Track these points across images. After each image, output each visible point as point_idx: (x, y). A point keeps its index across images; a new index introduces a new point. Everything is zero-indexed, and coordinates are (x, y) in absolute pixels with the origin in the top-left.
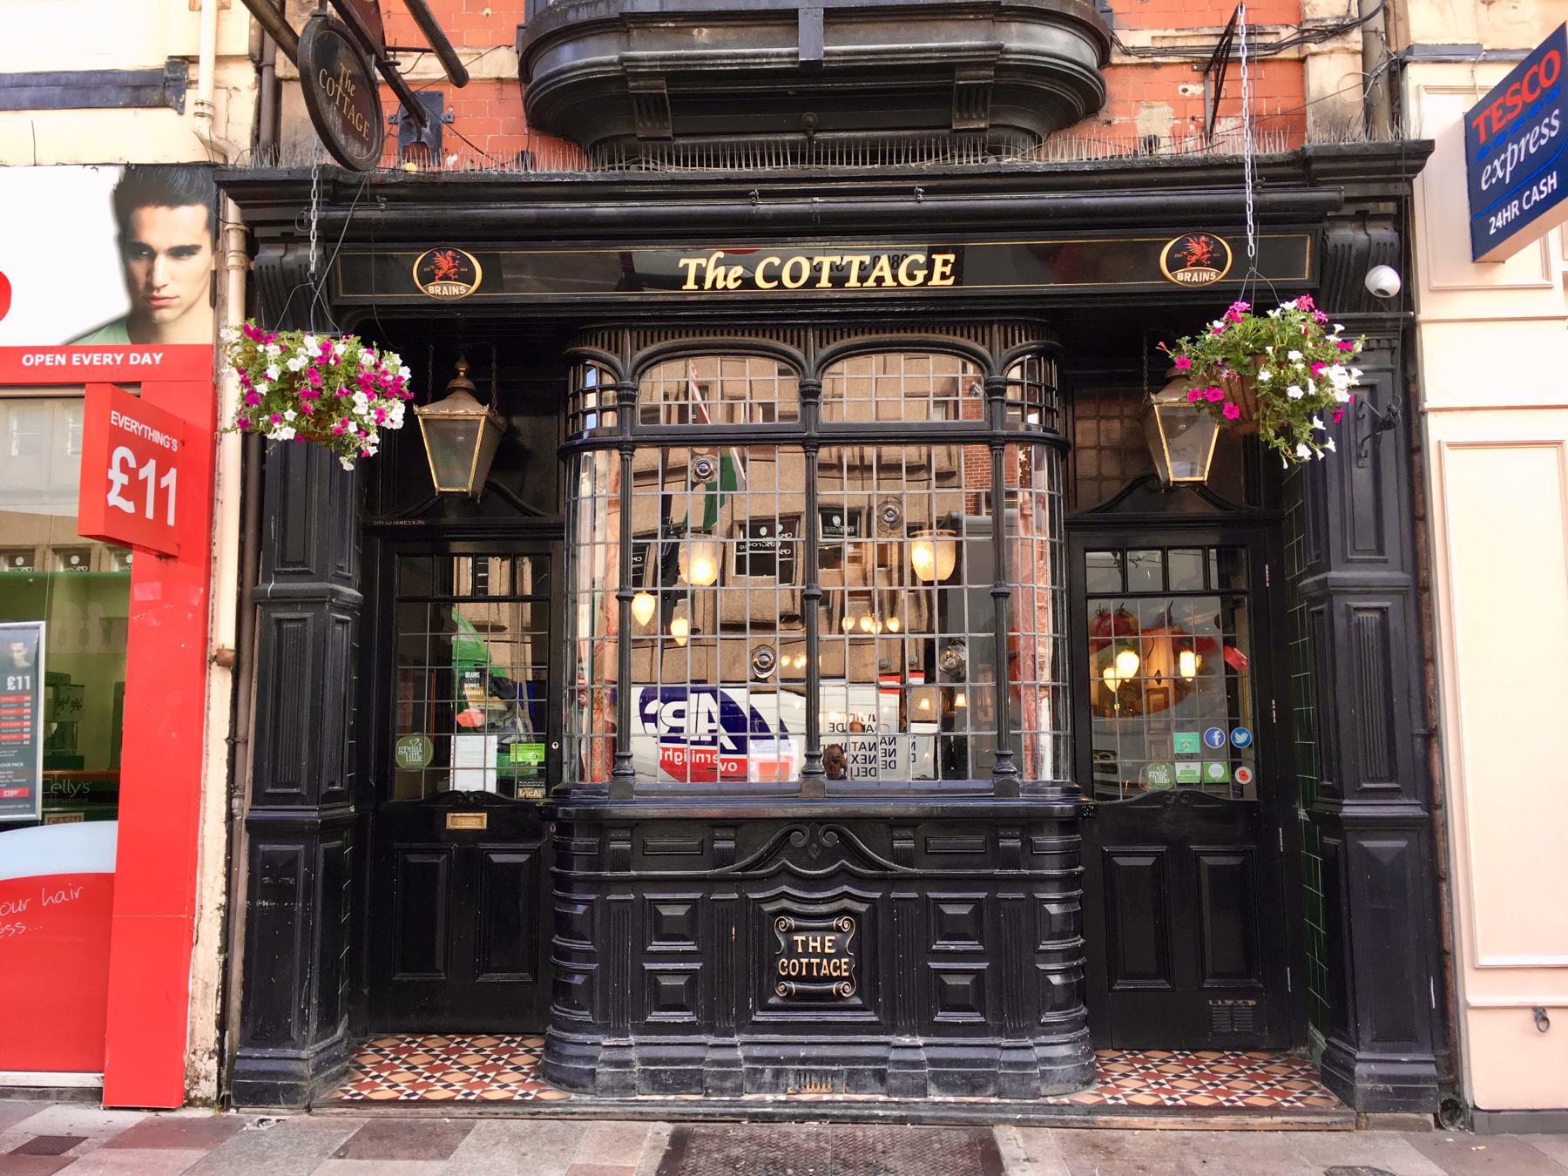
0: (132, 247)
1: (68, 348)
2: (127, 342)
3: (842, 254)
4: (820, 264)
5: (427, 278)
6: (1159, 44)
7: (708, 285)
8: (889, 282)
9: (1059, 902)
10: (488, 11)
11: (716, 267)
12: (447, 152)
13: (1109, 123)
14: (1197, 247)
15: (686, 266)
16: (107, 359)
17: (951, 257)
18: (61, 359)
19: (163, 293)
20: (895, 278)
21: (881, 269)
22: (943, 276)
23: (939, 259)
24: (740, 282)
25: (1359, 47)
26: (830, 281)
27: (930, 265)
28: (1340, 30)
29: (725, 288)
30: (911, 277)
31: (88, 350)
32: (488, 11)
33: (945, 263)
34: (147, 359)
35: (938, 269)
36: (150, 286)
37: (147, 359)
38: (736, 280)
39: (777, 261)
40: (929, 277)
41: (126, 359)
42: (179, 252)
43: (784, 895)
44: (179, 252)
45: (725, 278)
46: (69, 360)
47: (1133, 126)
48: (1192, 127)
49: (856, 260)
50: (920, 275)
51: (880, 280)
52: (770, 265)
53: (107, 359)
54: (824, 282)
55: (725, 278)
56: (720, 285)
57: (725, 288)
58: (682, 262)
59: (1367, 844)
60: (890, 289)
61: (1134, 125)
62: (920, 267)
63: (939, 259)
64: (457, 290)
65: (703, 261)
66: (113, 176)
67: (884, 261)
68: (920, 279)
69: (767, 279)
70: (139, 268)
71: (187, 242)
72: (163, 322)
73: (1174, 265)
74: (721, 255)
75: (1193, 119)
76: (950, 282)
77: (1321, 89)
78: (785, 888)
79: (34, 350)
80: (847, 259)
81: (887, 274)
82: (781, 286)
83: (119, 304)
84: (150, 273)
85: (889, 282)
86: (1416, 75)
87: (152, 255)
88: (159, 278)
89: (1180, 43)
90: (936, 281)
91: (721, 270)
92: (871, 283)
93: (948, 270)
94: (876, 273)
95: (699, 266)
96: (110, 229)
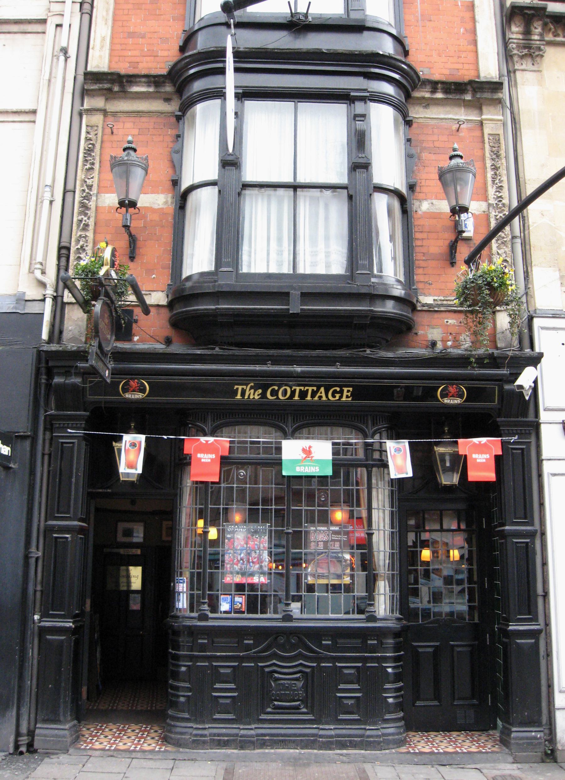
3: (304, 386)
4: (295, 390)
5: (125, 390)
7: (246, 397)
8: (324, 398)
9: (393, 668)
10: (154, 276)
11: (250, 390)
12: (134, 335)
13: (416, 334)
14: (452, 389)
15: (238, 389)
17: (351, 389)
20: (327, 396)
21: (321, 393)
22: (347, 397)
23: (345, 389)
24: (260, 396)
26: (299, 397)
27: (341, 392)
29: (254, 398)
30: (334, 396)
32: (154, 276)
33: (348, 391)
35: (345, 393)
38: (258, 395)
39: (276, 388)
40: (341, 397)
43: (274, 665)
45: (254, 395)
47: (426, 335)
48: (450, 337)
49: (310, 389)
50: (338, 396)
51: (320, 397)
52: (274, 389)
54: (296, 398)
55: (254, 395)
56: (251, 397)
57: (254, 398)
58: (236, 387)
59: (518, 641)
60: (325, 401)
61: (427, 335)
62: (338, 393)
63: (345, 389)
64: (139, 396)
65: (245, 387)
67: (322, 389)
68: (337, 398)
69: (272, 395)
73: (443, 396)
74: (252, 384)
75: (451, 334)
76: (350, 399)
78: (274, 661)
80: (306, 388)
81: (323, 395)
82: (278, 398)
85: (324, 398)
86: (537, 322)
89: (445, 302)
90: (344, 399)
91: (252, 391)
92: (316, 398)
93: (349, 394)
94: (319, 394)
95: (243, 389)
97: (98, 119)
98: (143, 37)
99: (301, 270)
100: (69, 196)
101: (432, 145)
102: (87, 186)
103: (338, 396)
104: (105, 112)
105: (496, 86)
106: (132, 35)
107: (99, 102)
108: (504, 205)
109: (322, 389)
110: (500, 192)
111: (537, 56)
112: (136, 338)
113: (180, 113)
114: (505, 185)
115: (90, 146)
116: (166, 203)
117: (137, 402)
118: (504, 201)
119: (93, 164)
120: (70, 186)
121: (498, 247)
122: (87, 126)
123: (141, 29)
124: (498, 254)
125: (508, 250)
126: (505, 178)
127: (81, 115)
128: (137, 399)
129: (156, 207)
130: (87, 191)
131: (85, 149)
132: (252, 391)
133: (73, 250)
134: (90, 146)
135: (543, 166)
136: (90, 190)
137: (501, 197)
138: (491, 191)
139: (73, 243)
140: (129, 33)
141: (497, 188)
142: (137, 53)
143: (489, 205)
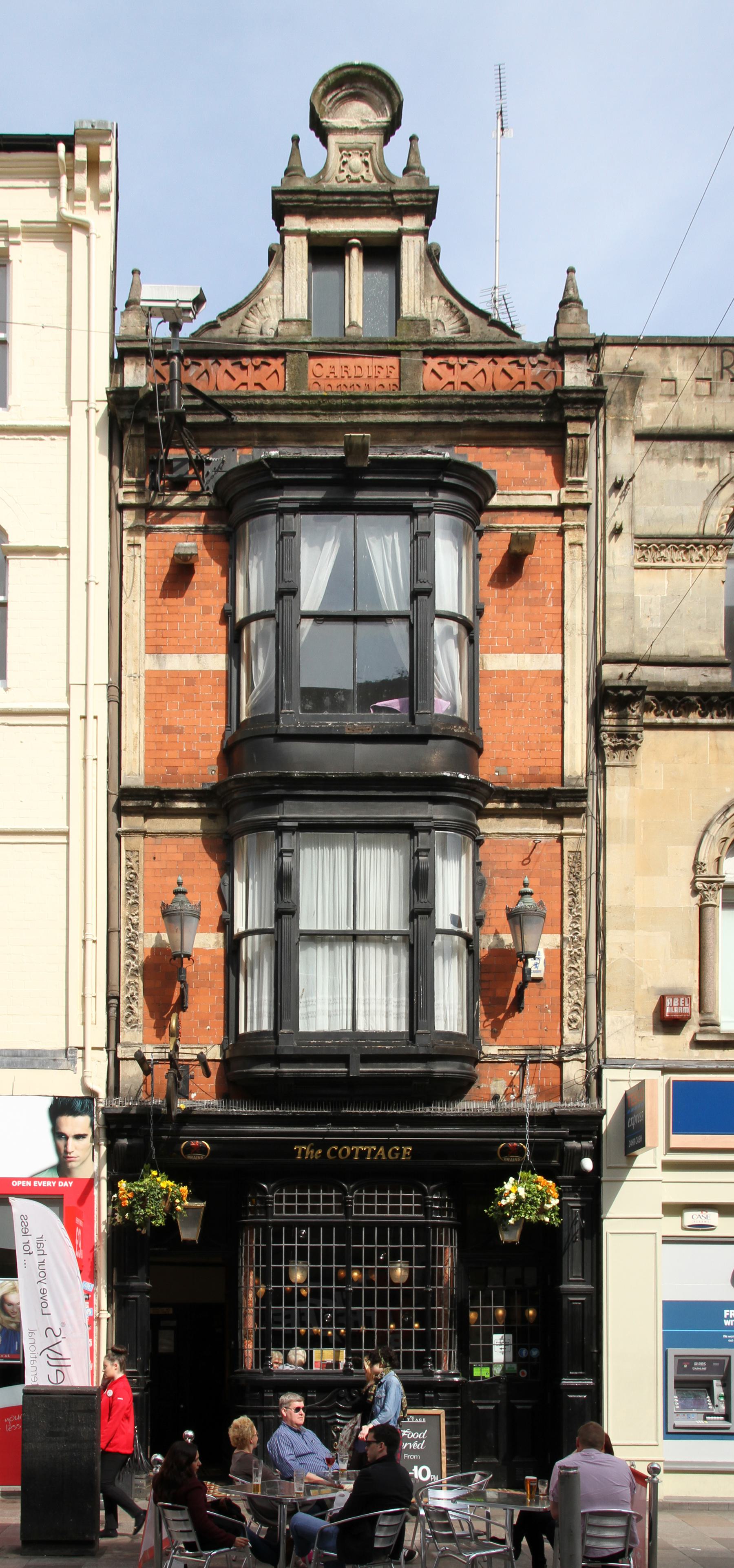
0: (58, 1134)
1: (31, 1179)
2: (57, 1176)
6: (501, 1052)
8: (384, 1158)
10: (208, 1027)
16: (49, 1184)
18: (29, 1183)
19: (72, 1155)
25: (585, 1059)
28: (577, 1051)
31: (40, 1180)
32: (208, 1027)
34: (66, 1184)
36: (66, 1152)
37: (66, 1184)
40: (401, 1156)
41: (57, 1184)
42: (78, 1137)
44: (78, 1137)
46: (32, 1184)
47: (489, 1089)
50: (397, 1155)
51: (380, 1156)
53: (49, 1184)
66: (49, 1102)
67: (381, 1149)
68: (397, 1157)
70: (61, 1143)
71: (82, 1133)
72: (72, 1168)
77: (568, 1076)
79: (17, 1179)
82: (338, 1157)
83: (54, 1160)
84: (66, 1146)
86: (607, 1074)
87: (67, 1138)
88: (70, 1149)
89: (510, 1052)
96: (48, 1125)
97: (137, 842)
98: (181, 732)
99: (361, 1027)
100: (114, 936)
101: (503, 867)
102: (133, 925)
103: (397, 1155)
104: (145, 834)
105: (580, 795)
106: (168, 730)
107: (137, 822)
108: (580, 938)
109: (381, 1149)
110: (575, 923)
111: (633, 746)
112: (193, 1096)
113: (61, 147)
114: (583, 915)
115: (132, 876)
116: (217, 943)
117: (199, 1162)
118: (580, 934)
119: (137, 898)
120: (114, 924)
121: (571, 989)
122: (127, 851)
123: (178, 722)
124: (570, 996)
125: (581, 991)
126: (583, 906)
127: (119, 837)
128: (199, 1161)
129: (208, 948)
130: (132, 930)
131: (126, 880)
132: (312, 1151)
133: (123, 999)
134: (132, 876)
135: (627, 889)
136: (137, 930)
137: (577, 929)
138: (567, 922)
139: (122, 992)
140: (164, 727)
141: (574, 918)
142: (176, 754)
143: (563, 939)
